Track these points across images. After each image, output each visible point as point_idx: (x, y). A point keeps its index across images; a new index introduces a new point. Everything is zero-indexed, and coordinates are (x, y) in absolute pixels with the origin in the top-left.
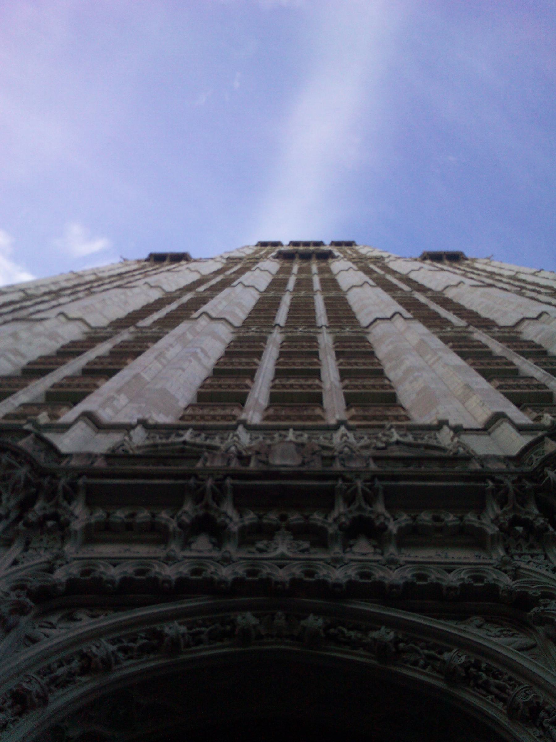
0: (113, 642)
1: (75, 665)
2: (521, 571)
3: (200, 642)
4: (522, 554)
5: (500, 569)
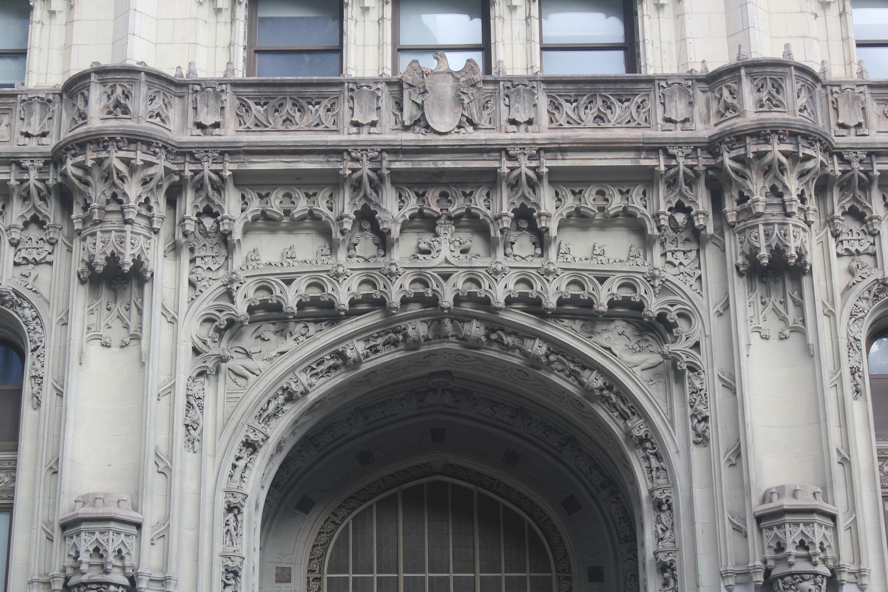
0: (305, 370)
1: (281, 399)
2: (666, 283)
3: (377, 351)
4: (676, 251)
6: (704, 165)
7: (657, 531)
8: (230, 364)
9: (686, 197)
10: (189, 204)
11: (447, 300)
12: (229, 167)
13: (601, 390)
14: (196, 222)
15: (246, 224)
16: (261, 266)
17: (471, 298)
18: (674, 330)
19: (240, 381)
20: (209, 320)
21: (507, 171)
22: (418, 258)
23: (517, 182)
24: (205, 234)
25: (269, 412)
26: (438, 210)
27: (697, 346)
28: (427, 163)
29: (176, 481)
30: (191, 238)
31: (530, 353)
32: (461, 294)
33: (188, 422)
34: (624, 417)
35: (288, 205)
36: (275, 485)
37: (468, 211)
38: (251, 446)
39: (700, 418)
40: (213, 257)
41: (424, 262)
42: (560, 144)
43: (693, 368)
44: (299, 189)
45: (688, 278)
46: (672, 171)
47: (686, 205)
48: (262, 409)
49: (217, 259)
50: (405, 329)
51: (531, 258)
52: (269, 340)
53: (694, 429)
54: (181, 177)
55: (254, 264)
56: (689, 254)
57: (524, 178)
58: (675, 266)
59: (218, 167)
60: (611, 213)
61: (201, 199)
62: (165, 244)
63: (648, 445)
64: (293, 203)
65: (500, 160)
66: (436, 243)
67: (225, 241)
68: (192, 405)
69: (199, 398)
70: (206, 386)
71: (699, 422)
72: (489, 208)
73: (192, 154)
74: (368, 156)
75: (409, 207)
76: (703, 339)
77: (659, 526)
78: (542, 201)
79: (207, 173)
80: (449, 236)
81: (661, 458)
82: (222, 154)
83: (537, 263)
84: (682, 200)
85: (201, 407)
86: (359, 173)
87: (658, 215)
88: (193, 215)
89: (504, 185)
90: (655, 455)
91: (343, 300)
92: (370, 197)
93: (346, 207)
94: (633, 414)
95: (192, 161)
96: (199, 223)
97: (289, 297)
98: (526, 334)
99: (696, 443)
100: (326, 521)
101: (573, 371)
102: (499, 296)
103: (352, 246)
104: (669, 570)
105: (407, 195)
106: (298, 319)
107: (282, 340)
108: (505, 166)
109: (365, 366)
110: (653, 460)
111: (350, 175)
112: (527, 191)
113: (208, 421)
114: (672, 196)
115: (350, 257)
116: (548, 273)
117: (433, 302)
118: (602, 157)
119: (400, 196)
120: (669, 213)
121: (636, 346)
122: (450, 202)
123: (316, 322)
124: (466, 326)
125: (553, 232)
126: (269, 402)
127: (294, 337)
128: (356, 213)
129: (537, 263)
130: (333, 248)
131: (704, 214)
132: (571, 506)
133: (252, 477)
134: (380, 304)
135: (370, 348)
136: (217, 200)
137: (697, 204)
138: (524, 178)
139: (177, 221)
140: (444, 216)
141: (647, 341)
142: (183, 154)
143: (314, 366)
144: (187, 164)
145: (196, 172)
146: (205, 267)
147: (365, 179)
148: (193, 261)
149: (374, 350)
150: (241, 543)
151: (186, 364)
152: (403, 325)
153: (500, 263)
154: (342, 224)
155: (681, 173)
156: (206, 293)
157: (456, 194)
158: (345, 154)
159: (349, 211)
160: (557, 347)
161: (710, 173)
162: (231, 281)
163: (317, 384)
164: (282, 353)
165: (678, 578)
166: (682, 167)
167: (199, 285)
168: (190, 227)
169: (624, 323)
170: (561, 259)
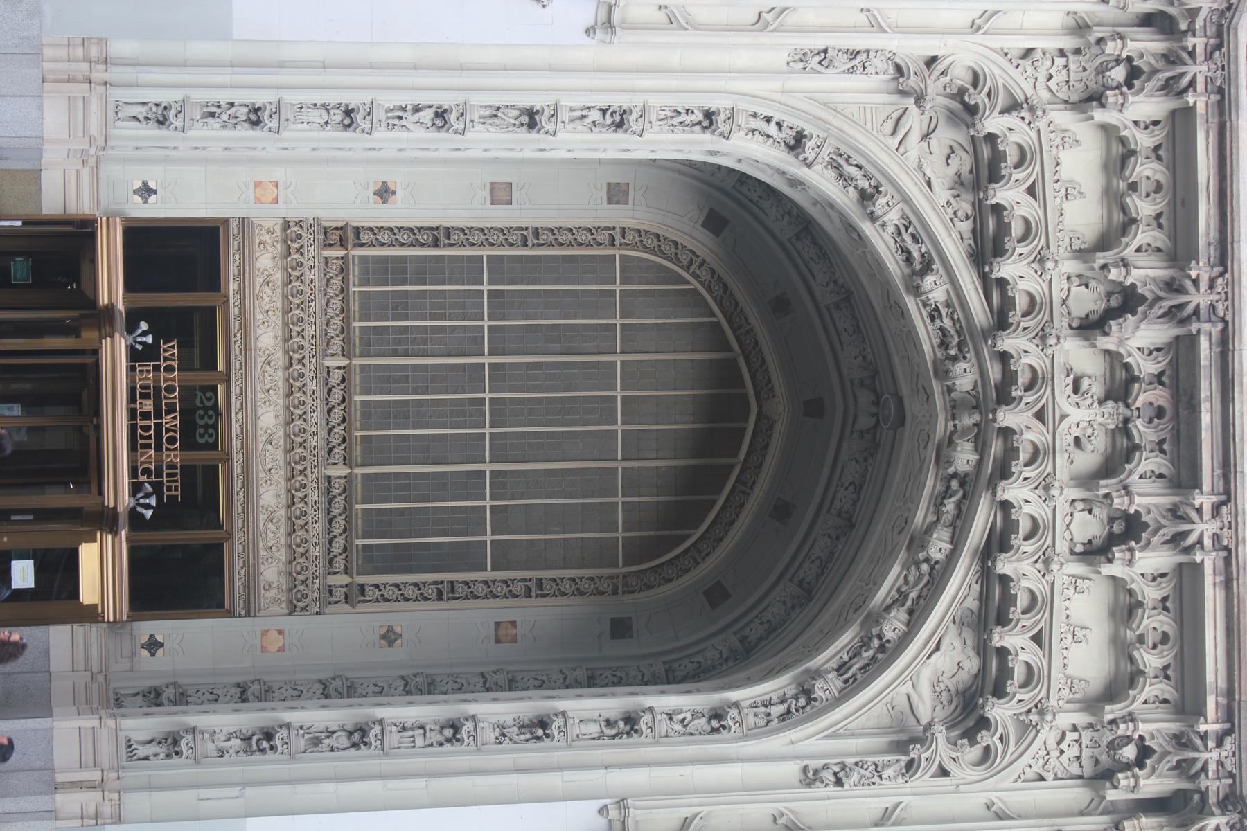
0: (904, 216)
1: (864, 184)
2: (1034, 732)
3: (932, 318)
4: (1080, 745)
5: (1036, 706)
6: (1207, 788)
7: (681, 712)
8: (914, 110)
9: (1160, 761)
10: (1146, 45)
11: (1006, 417)
12: (1199, 101)
13: (880, 637)
14: (1119, 56)
15: (1116, 128)
16: (1054, 151)
17: (1010, 452)
18: (965, 741)
19: (889, 126)
20: (976, 80)
21: (1197, 503)
22: (1068, 375)
23: (1181, 518)
24: (1101, 70)
25: (846, 166)
26: (1138, 404)
27: (944, 773)
28: (1208, 387)
29: (746, 39)
30: (1095, 50)
31: (931, 536)
32: (1015, 437)
33: (830, 53)
34: (841, 669)
35: (1144, 187)
36: (743, 178)
37: (1136, 448)
38: (797, 143)
39: (841, 775)
40: (1067, 82)
41: (1063, 385)
42: (1238, 579)
43: (910, 766)
44: (1169, 203)
45: (1041, 762)
46: (1198, 742)
47: (1148, 762)
48: (850, 157)
49: (1065, 89)
50: (965, 358)
51: (1069, 538)
52: (948, 164)
53: (825, 767)
54: (1185, 32)
55: (1058, 141)
56: (1076, 764)
57: (1186, 527)
58: (1059, 743)
59: (1200, 86)
60: (1135, 653)
61: (1153, 62)
62: (1086, 13)
63: (802, 701)
64: (1148, 195)
65: (1213, 492)
66: (1089, 401)
67: (1094, 98)
68: (855, 58)
69: (864, 68)
70: (881, 77)
71: (835, 774)
72: (1141, 477)
73: (1219, 47)
74: (1217, 301)
75: (1141, 362)
76: (954, 782)
77: (688, 716)
78: (1152, 554)
79: (1191, 69)
80: (1100, 419)
81: (783, 720)
82: (1220, 91)
83: (1062, 546)
84: (1156, 756)
85: (851, 70)
86: (1192, 289)
87: (1132, 720)
88: (1129, 51)
89: (1176, 499)
90: (789, 712)
91: (1006, 269)
92: (1157, 306)
93: (1142, 272)
94: (846, 681)
95: (1209, 49)
96: (1118, 61)
97: (1010, 192)
98: (958, 530)
99: (805, 769)
100: (693, 252)
101: (907, 596)
102: (1012, 491)
103: (1084, 281)
104: (628, 728)
105: (1160, 359)
106: (978, 206)
107: (948, 182)
108: (1204, 499)
109: (911, 303)
110: (780, 709)
111: (1189, 277)
112: (1168, 532)
113: (832, 82)
114: (1161, 740)
115: (1068, 278)
116: (1047, 562)
117: (1004, 397)
118: (1218, 641)
119: (1158, 350)
120: (1136, 736)
121: (942, 686)
122: (1151, 421)
123: (974, 231)
124: (969, 446)
125: (1107, 569)
126: (859, 167)
127: (952, 201)
128: (1133, 285)
129: (1062, 546)
130: (1082, 254)
131: (1134, 787)
132: (716, 595)
133: (755, 146)
134: (1001, 322)
135: (937, 309)
136: (1150, 85)
137: (1149, 776)
138: (1186, 527)
139: (1119, 29)
140: (1128, 413)
141: (950, 702)
142: (1219, 34)
143: (910, 230)
144: (1205, 40)
145: (1192, 54)
146: (1052, 71)
147: (1183, 299)
148: (1062, 53)
149: (935, 315)
150: (661, 131)
151: (912, 49)
152: (971, 355)
153: (1061, 493)
154: (1116, 265)
155: (1195, 755)
156: (1015, 74)
157: (1162, 430)
158: (1221, 269)
159: (1135, 276)
160: (938, 576)
161: (1196, 797)
162: (1032, 109)
163: (885, 235)
164: (929, 183)
165: (617, 741)
166: (1204, 755)
167: (1026, 63)
168: (1112, 48)
169: (975, 669)
170: (1067, 580)
